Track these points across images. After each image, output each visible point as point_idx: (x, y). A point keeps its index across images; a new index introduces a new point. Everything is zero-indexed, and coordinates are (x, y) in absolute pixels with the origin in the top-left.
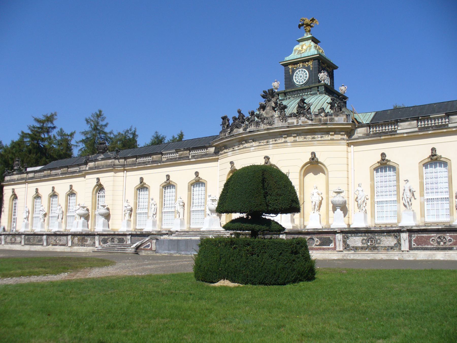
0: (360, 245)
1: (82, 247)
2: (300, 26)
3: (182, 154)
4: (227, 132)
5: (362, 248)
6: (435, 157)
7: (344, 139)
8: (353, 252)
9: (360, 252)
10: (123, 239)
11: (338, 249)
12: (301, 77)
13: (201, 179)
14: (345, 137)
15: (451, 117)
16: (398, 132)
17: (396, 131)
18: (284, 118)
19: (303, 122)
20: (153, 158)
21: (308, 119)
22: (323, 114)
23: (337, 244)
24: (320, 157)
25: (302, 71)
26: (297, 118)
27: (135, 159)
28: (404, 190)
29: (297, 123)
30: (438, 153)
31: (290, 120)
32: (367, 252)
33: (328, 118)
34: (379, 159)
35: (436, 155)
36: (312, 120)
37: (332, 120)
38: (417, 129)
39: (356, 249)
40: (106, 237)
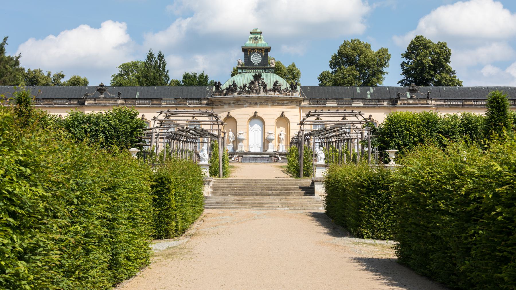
12: (256, 58)
16: (327, 105)
17: (325, 104)
18: (266, 91)
19: (277, 95)
22: (288, 91)
24: (286, 115)
25: (257, 55)
31: (270, 93)
33: (291, 93)
36: (282, 94)
37: (292, 95)
38: (336, 105)
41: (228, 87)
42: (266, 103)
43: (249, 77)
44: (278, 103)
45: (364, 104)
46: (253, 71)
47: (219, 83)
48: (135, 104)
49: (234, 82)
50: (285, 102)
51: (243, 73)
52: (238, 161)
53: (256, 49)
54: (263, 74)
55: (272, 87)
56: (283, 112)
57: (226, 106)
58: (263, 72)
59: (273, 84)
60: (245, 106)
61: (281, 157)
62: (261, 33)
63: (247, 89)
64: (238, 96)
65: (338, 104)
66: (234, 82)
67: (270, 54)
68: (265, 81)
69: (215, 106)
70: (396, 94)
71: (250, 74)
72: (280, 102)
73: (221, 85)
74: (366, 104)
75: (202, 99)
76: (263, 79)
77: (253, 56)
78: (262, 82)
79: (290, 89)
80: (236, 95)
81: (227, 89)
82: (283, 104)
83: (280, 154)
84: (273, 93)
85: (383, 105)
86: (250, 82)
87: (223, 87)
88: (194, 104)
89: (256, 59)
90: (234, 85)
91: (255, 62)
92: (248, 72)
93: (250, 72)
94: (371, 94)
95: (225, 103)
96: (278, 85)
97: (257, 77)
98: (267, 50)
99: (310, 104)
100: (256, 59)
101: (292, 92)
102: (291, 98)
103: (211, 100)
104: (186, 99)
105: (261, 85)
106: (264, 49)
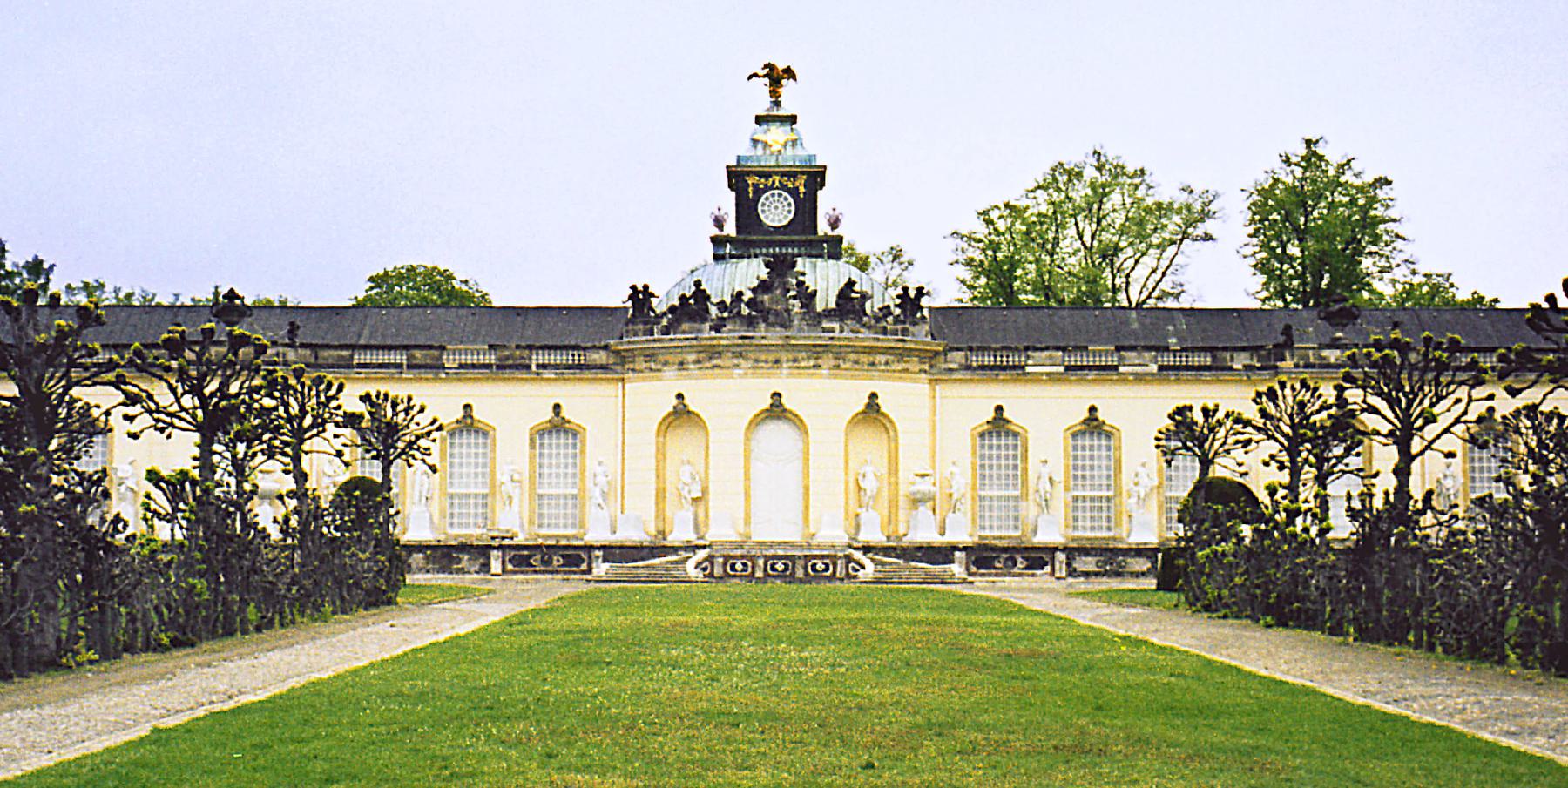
0: (1092, 568)
1: (441, 576)
2: (756, 75)
3: (507, 358)
4: (659, 323)
5: (1097, 574)
6: (1095, 423)
7: (925, 372)
8: (1082, 579)
9: (1093, 579)
10: (579, 556)
11: (1057, 575)
12: (776, 208)
13: (569, 422)
14: (926, 367)
15: (1123, 353)
16: (1028, 369)
17: (1023, 368)
18: (814, 317)
20: (413, 357)
21: (864, 325)
22: (890, 319)
23: (1057, 566)
25: (780, 195)
26: (841, 320)
27: (345, 353)
28: (1039, 478)
29: (842, 331)
30: (1100, 415)
31: (826, 324)
32: (1105, 579)
33: (899, 327)
34: (991, 415)
35: (1096, 419)
36: (869, 328)
38: (1061, 369)
39: (1087, 574)
40: (526, 553)
41: (677, 303)
42: (812, 363)
43: (751, 271)
44: (856, 362)
45: (1161, 368)
46: (764, 251)
47: (646, 287)
48: (350, 366)
49: (698, 284)
50: (881, 358)
51: (732, 257)
52: (712, 575)
53: (776, 173)
54: (799, 260)
55: (832, 305)
56: (873, 396)
57: (670, 372)
58: (799, 255)
59: (837, 292)
60: (737, 371)
61: (873, 560)
62: (792, 119)
63: (745, 311)
64: (713, 334)
65: (1068, 368)
66: (698, 284)
67: (826, 201)
68: (809, 281)
69: (631, 375)
70: (1280, 327)
71: (754, 261)
72: (864, 358)
73: (652, 295)
74: (1168, 368)
75: (585, 349)
76: (803, 274)
77: (767, 199)
78: (800, 284)
79: (897, 311)
80: (706, 332)
81: (672, 309)
82: (873, 364)
83: (867, 549)
84: (836, 326)
85: (1231, 368)
86: (755, 283)
87: (659, 305)
88: (556, 367)
89: (776, 211)
90: (701, 295)
91: (773, 220)
92: (749, 257)
93: (756, 256)
94: (1176, 334)
95: (666, 364)
96: (853, 295)
97: (781, 267)
98: (817, 177)
99: (968, 368)
100: (776, 211)
101: (904, 322)
102: (900, 345)
103: (618, 352)
104: (530, 347)
105: (794, 298)
106: (803, 173)
